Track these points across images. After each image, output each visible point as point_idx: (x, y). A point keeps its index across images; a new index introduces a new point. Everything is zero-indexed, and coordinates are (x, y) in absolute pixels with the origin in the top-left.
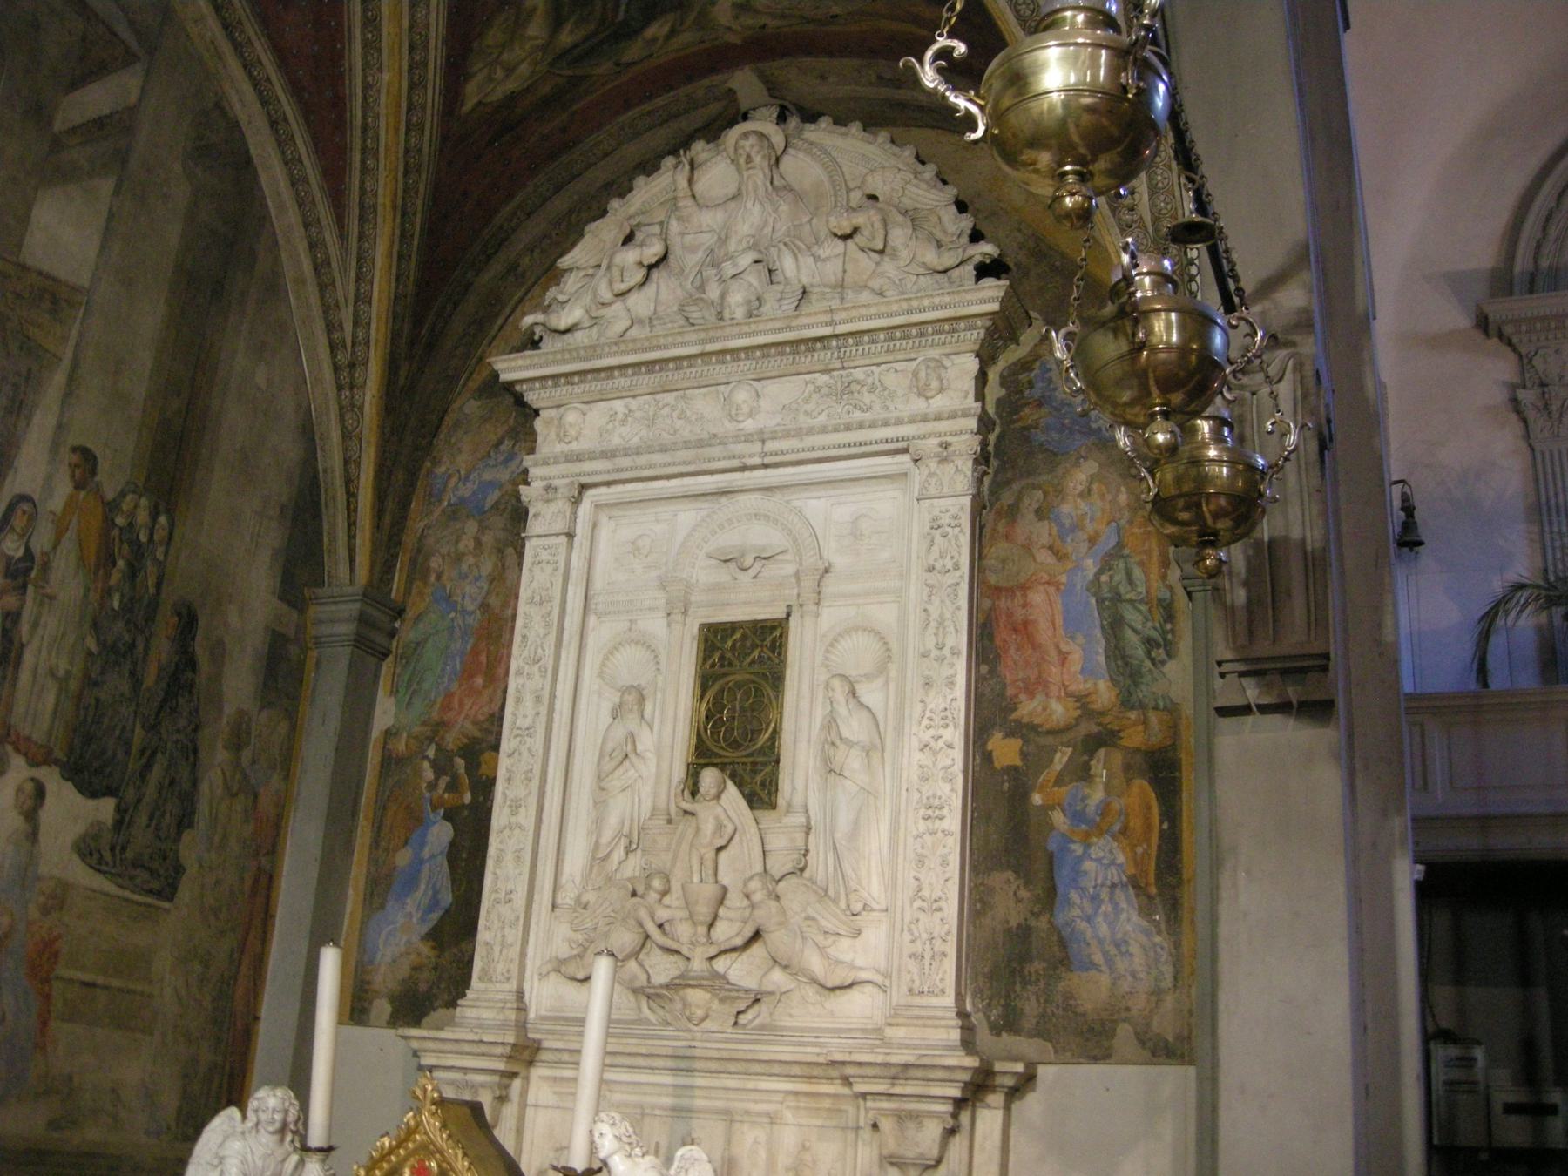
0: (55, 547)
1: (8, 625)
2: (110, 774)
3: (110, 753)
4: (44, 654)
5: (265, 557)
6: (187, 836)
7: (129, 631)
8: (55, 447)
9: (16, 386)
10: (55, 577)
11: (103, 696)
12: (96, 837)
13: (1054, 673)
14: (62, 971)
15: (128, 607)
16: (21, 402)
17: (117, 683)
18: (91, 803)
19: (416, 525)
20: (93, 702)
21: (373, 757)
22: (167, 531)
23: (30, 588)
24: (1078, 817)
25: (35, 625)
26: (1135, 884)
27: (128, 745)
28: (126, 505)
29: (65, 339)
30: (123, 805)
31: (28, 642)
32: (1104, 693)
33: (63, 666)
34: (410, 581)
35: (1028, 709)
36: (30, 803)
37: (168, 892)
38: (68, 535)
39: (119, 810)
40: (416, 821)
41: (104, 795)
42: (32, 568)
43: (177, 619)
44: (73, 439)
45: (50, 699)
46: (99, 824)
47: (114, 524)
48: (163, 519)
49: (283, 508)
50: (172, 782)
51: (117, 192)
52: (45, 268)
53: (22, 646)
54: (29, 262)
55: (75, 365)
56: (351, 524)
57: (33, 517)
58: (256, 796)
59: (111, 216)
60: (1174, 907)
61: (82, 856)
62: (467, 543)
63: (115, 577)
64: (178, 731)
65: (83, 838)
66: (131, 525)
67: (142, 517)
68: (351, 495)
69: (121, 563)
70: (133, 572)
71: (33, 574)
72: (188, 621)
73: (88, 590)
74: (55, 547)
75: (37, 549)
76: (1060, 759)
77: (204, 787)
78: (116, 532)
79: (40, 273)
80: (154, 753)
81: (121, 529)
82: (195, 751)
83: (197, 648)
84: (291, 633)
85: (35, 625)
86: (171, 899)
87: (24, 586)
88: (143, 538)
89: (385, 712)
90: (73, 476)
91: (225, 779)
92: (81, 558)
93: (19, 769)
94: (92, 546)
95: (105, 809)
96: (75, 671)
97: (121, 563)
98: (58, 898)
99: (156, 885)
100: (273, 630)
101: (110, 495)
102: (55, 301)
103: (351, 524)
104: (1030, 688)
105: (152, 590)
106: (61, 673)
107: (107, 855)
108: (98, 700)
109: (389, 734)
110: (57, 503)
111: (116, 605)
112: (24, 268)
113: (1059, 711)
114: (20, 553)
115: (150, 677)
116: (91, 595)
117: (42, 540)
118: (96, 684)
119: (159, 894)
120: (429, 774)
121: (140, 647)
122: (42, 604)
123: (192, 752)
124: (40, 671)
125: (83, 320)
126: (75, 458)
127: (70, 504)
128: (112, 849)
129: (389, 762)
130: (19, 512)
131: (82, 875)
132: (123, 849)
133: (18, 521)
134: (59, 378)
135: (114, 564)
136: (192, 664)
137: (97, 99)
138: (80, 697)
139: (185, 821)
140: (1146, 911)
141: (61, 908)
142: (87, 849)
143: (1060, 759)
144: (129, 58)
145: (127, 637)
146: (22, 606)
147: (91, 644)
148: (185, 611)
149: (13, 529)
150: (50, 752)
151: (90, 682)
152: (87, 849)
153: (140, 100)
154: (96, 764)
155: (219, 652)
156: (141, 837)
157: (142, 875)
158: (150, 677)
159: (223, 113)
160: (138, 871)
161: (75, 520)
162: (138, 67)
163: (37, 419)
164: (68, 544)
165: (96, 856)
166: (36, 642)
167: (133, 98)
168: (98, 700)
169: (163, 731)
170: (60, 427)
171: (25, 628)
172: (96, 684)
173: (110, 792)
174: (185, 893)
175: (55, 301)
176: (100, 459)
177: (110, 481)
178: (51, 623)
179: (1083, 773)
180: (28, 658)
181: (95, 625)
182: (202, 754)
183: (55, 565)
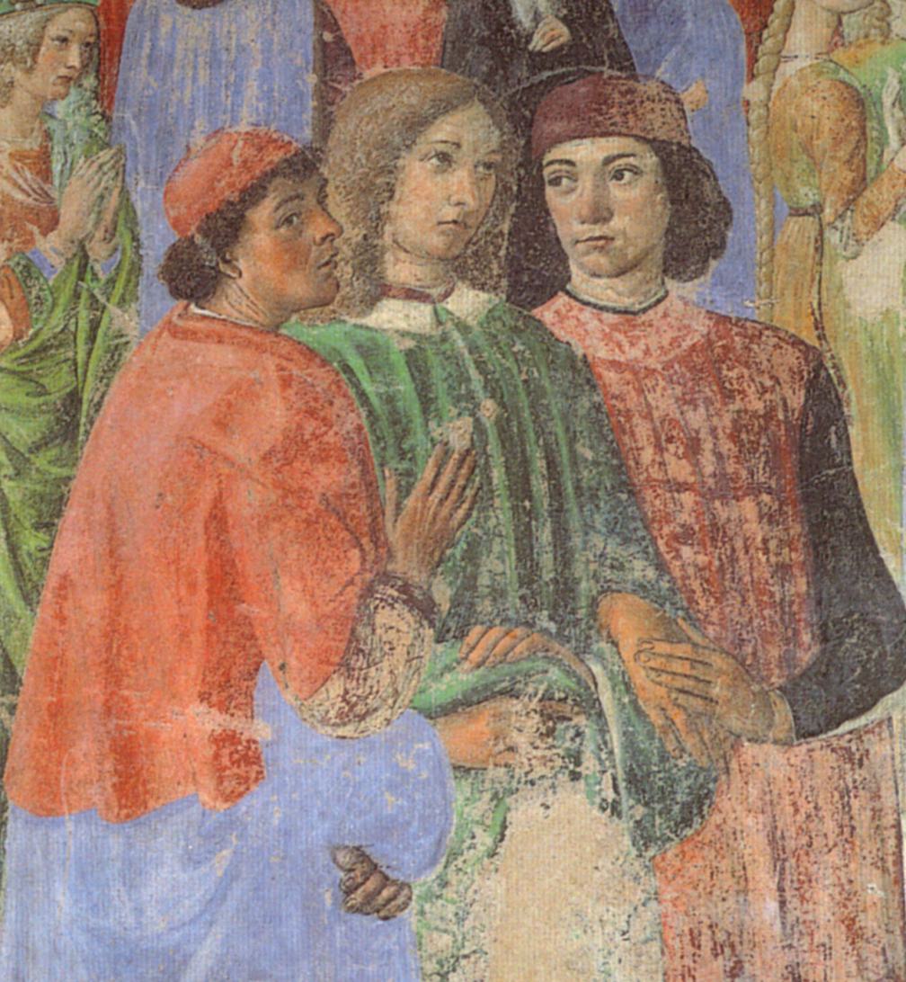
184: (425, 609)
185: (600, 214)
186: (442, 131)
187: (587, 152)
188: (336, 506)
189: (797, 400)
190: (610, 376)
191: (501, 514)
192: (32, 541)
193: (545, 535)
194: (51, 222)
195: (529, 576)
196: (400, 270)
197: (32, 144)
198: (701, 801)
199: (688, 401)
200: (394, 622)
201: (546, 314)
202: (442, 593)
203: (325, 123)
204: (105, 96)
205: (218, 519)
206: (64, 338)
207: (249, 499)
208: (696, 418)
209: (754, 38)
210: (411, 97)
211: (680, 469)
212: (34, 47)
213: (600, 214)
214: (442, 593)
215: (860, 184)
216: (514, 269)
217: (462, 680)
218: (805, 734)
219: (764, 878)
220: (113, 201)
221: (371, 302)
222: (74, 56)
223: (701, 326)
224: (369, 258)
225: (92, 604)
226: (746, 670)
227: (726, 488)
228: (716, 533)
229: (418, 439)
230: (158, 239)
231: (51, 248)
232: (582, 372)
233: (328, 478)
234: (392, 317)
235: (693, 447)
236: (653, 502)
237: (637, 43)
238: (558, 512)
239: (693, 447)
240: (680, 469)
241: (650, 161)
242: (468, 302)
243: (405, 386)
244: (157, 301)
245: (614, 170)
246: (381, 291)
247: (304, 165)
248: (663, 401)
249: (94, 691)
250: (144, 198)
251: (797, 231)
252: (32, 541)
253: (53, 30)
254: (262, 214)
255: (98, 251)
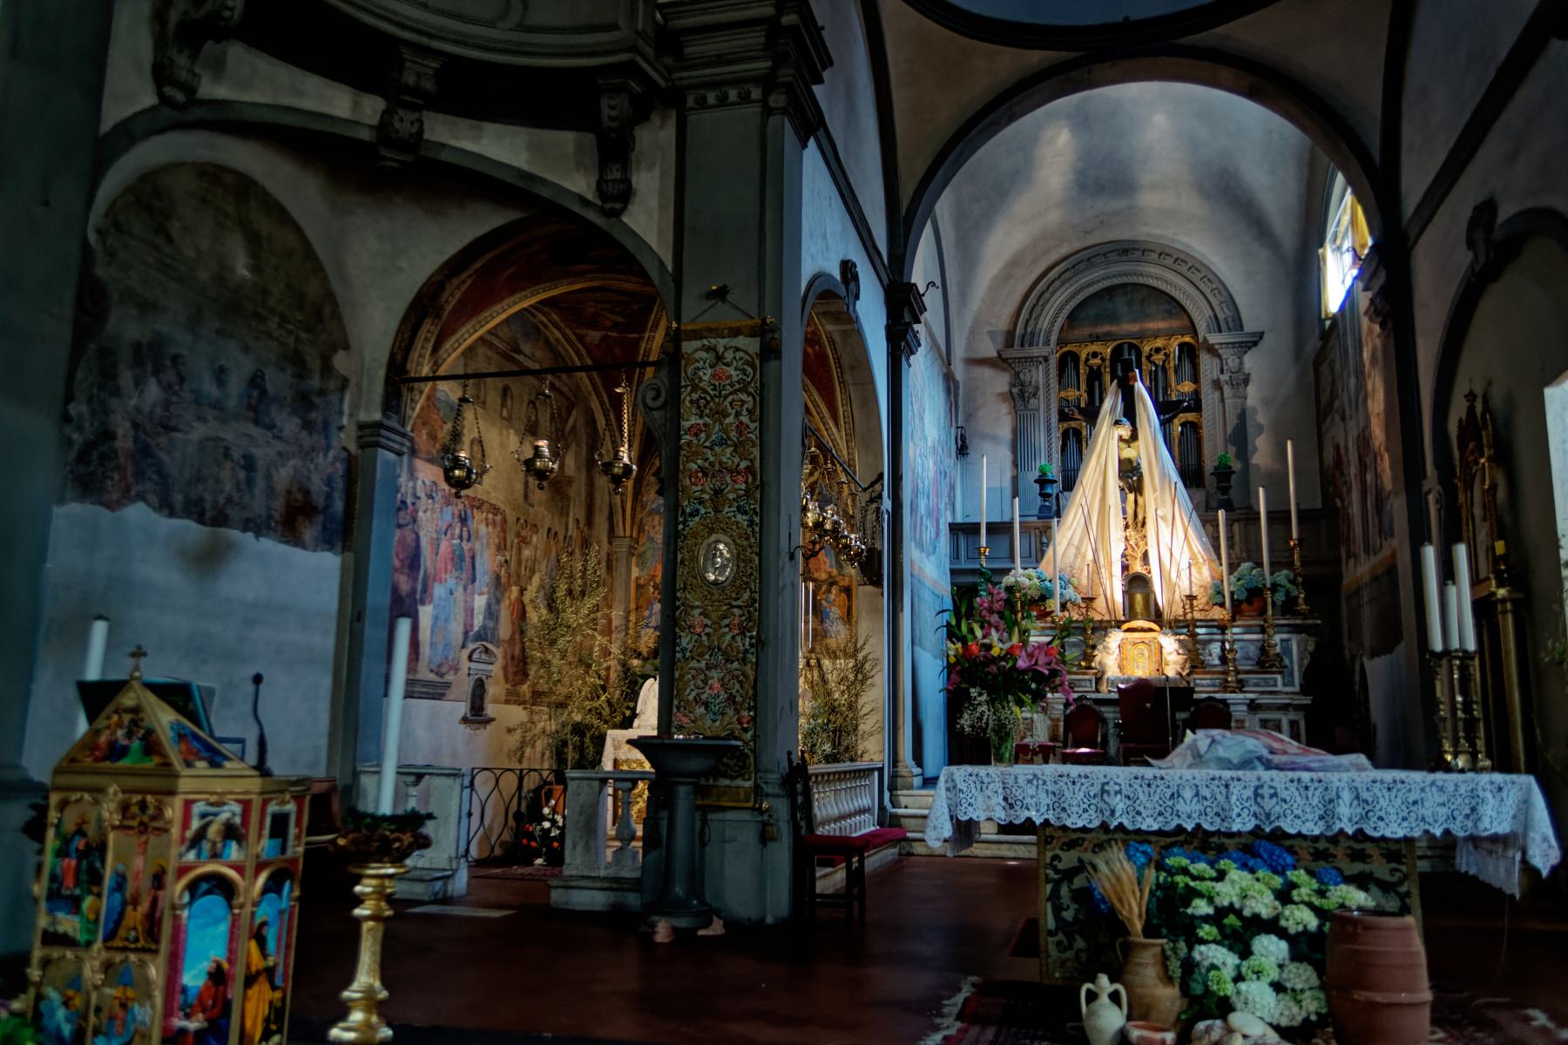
13: (822, 566)
19: (639, 516)
21: (633, 585)
24: (829, 602)
26: (842, 618)
32: (835, 572)
34: (639, 533)
35: (816, 575)
40: (650, 604)
56: (624, 519)
60: (850, 624)
62: (656, 523)
68: (624, 512)
76: (824, 588)
89: (635, 572)
103: (624, 519)
104: (817, 570)
109: (637, 578)
113: (823, 576)
120: (652, 590)
129: (638, 587)
140: (845, 624)
143: (824, 588)
179: (829, 591)
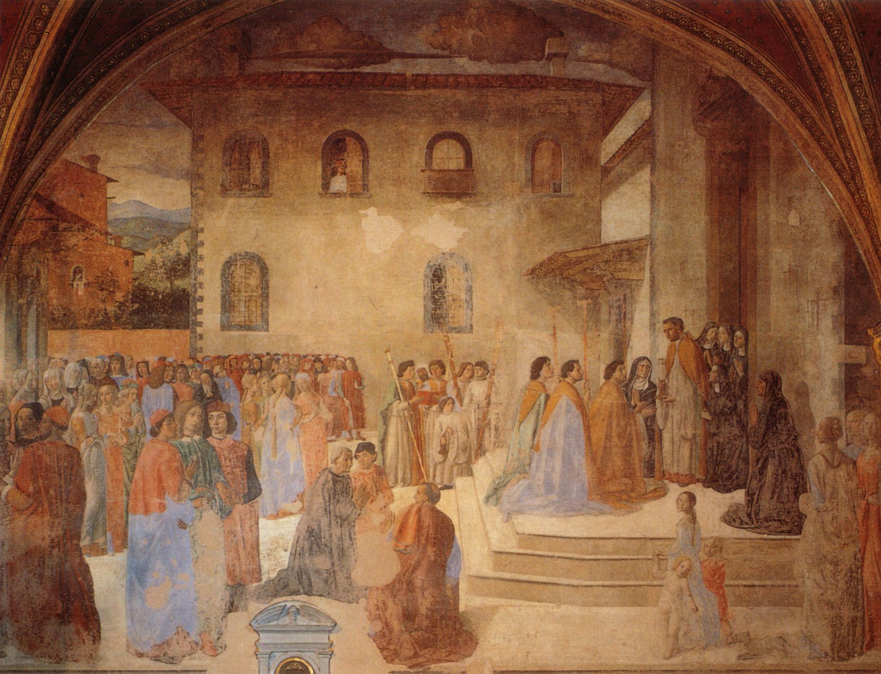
0: (668, 375)
1: (649, 424)
2: (737, 478)
3: (734, 468)
4: (676, 430)
5: (827, 323)
6: (802, 498)
7: (731, 401)
8: (653, 325)
9: (619, 307)
10: (672, 392)
11: (721, 440)
12: (735, 512)
14: (727, 582)
15: (726, 388)
16: (625, 313)
17: (729, 430)
18: (728, 495)
20: (715, 444)
22: (743, 339)
23: (657, 401)
25: (666, 417)
27: (746, 461)
28: (710, 335)
29: (642, 269)
30: (751, 492)
31: (664, 428)
33: (690, 433)
36: (686, 505)
37: (797, 528)
38: (674, 366)
39: (748, 494)
41: (735, 489)
42: (656, 391)
43: (764, 384)
44: (663, 317)
45: (685, 451)
46: (738, 505)
47: (703, 349)
48: (738, 333)
49: (835, 291)
50: (784, 472)
51: (652, 173)
52: (618, 239)
53: (661, 430)
54: (607, 242)
55: (653, 279)
57: (649, 367)
58: (855, 463)
59: (652, 187)
61: (729, 523)
63: (712, 375)
64: (782, 443)
65: (728, 513)
66: (716, 345)
67: (723, 337)
69: (715, 368)
70: (724, 369)
71: (658, 393)
72: (773, 381)
73: (695, 393)
74: (668, 375)
75: (655, 379)
77: (811, 469)
78: (706, 353)
79: (616, 243)
80: (766, 459)
81: (710, 350)
82: (798, 450)
83: (784, 395)
84: (862, 359)
85: (666, 417)
86: (800, 533)
87: (654, 401)
88: (726, 348)
90: (669, 336)
91: (827, 460)
92: (687, 376)
93: (675, 491)
94: (692, 366)
95: (739, 496)
96: (698, 432)
97: (715, 368)
98: (718, 545)
99: (785, 528)
100: (846, 364)
101: (696, 335)
102: (630, 252)
105: (741, 374)
106: (690, 436)
107: (746, 519)
108: (718, 443)
110: (663, 353)
111: (717, 390)
112: (606, 245)
114: (647, 386)
115: (753, 419)
116: (699, 392)
117: (657, 375)
118: (715, 434)
119: (789, 532)
121: (741, 406)
122: (667, 406)
123: (796, 452)
124: (675, 439)
125: (651, 255)
126: (667, 326)
127: (671, 351)
128: (749, 515)
130: (640, 367)
131: (728, 532)
132: (757, 514)
133: (641, 372)
134: (644, 291)
135: (710, 369)
136: (783, 403)
137: (623, 130)
138: (706, 444)
139: (800, 487)
141: (721, 552)
142: (730, 518)
144: (637, 92)
145: (729, 404)
146: (655, 412)
147: (706, 415)
148: (769, 377)
149: (639, 377)
150: (693, 476)
151: (709, 435)
152: (730, 518)
153: (653, 111)
154: (726, 475)
155: (803, 392)
156: (767, 504)
157: (774, 525)
158: (753, 419)
159: (716, 79)
160: (770, 523)
161: (677, 357)
162: (646, 94)
163: (637, 317)
164: (676, 371)
165: (738, 521)
166: (669, 424)
167: (647, 114)
168: (718, 443)
169: (770, 445)
170: (653, 314)
171: (660, 421)
172: (715, 434)
173: (738, 487)
174: (809, 527)
175: (630, 252)
176: (684, 320)
177: (693, 327)
178: (675, 413)
180: (666, 436)
181: (706, 405)
182: (804, 451)
183: (670, 384)
184: (190, 484)
185: (217, 424)
186: (193, 410)
187: (215, 414)
188: (177, 469)
189: (246, 453)
190: (217, 449)
191: (201, 470)
192: (131, 474)
193: (208, 473)
194: (132, 424)
195: (205, 480)
196: (186, 432)
197: (129, 411)
198: (230, 512)
199: (229, 453)
200: (186, 487)
201: (208, 439)
202: (193, 482)
203: (175, 408)
204: (140, 403)
205: (159, 471)
206: (135, 442)
207: (163, 468)
208: (231, 456)
209: (242, 395)
210: (186, 405)
211: (228, 464)
212: (128, 395)
213: (217, 424)
214: (193, 482)
215: (256, 421)
216: (204, 433)
217: (196, 495)
218: (245, 503)
219: (239, 523)
220: (142, 421)
221: (182, 437)
222: (135, 396)
223: (232, 442)
224: (182, 430)
225: (140, 484)
226: (237, 494)
227: (235, 467)
228: (233, 473)
229: (189, 459)
230: (149, 427)
231: (132, 429)
232: (214, 448)
233: (176, 464)
234: (186, 440)
235: (230, 460)
236: (224, 469)
237: (223, 396)
238: (210, 470)
239: (230, 460)
240: (228, 464)
241: (225, 415)
242: (197, 437)
243: (187, 451)
244: (148, 436)
245: (219, 417)
246: (183, 436)
247: (171, 415)
248: (226, 453)
249: (140, 497)
250: (147, 420)
251: (247, 427)
252: (131, 474)
253: (131, 392)
254: (165, 423)
255: (139, 428)
